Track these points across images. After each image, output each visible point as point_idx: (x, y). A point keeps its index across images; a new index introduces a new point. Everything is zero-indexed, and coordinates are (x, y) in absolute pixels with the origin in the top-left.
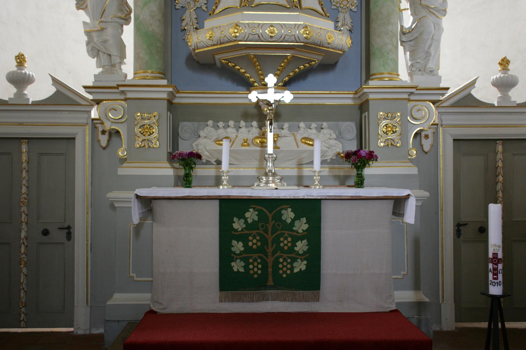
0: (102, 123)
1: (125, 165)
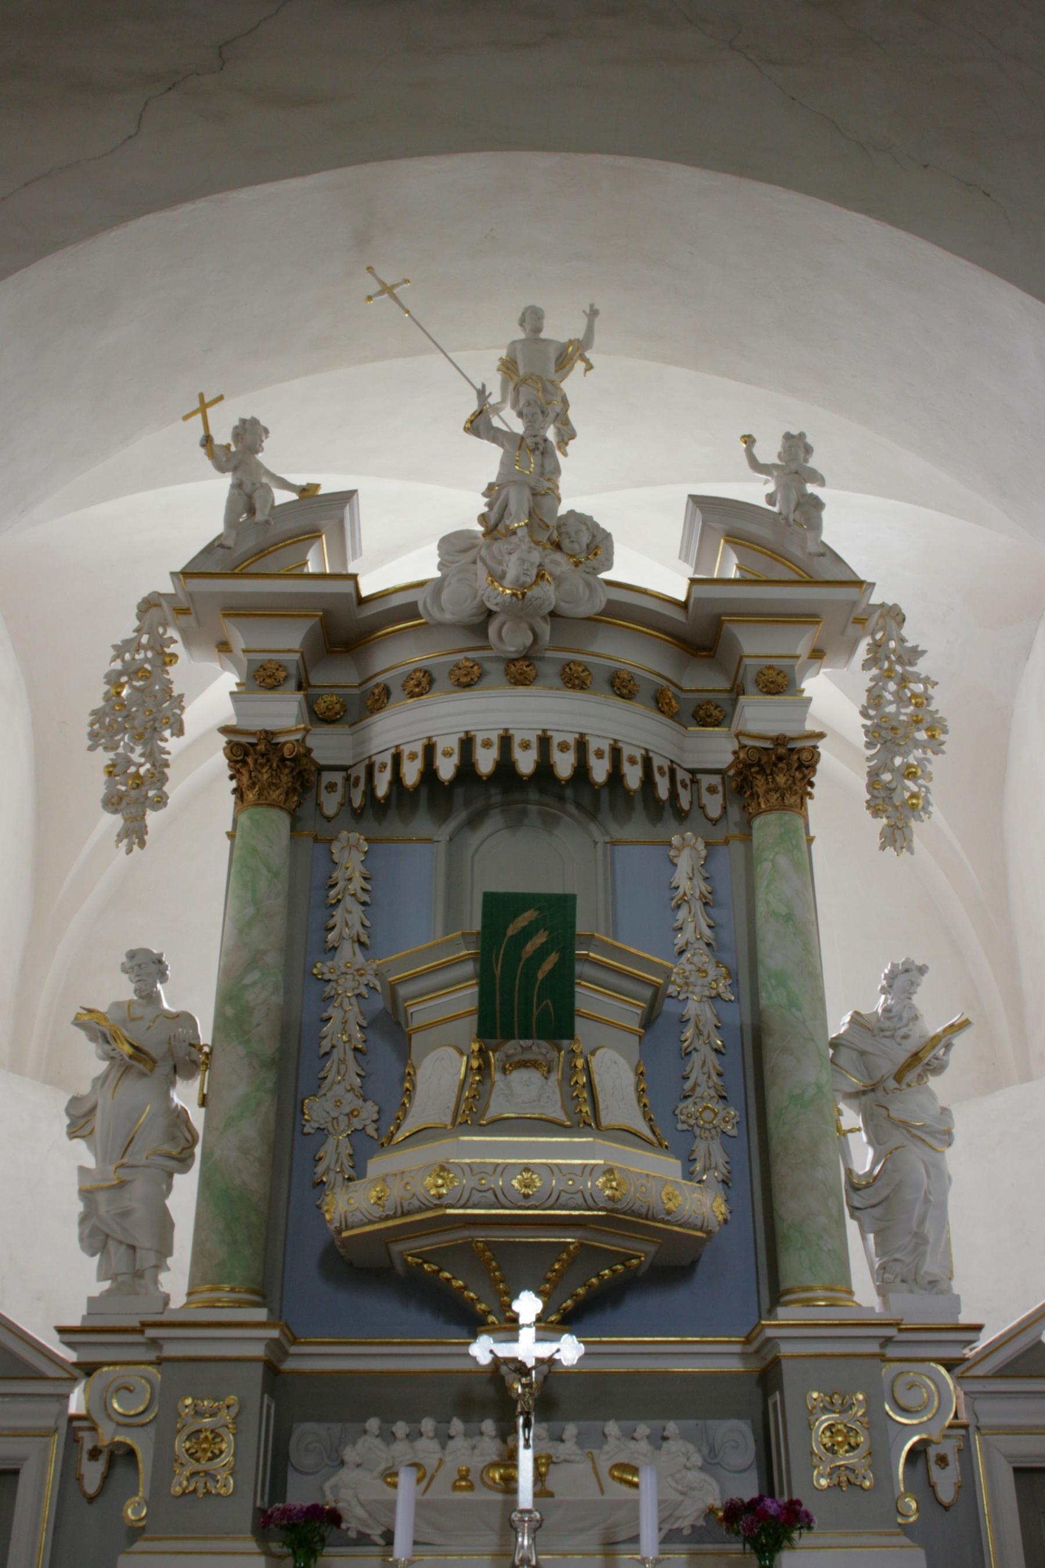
0: (93, 1429)
1: (140, 1545)
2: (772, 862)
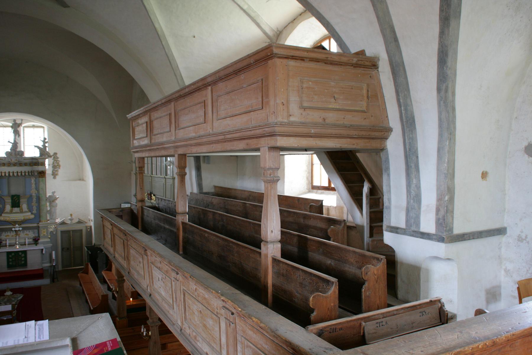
2: (41, 183)
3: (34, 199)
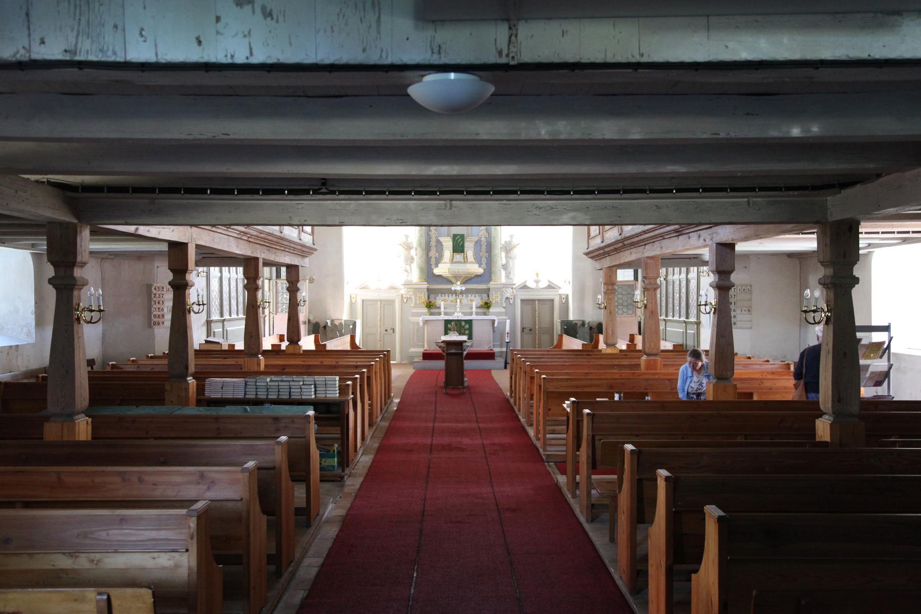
3: (484, 247)
